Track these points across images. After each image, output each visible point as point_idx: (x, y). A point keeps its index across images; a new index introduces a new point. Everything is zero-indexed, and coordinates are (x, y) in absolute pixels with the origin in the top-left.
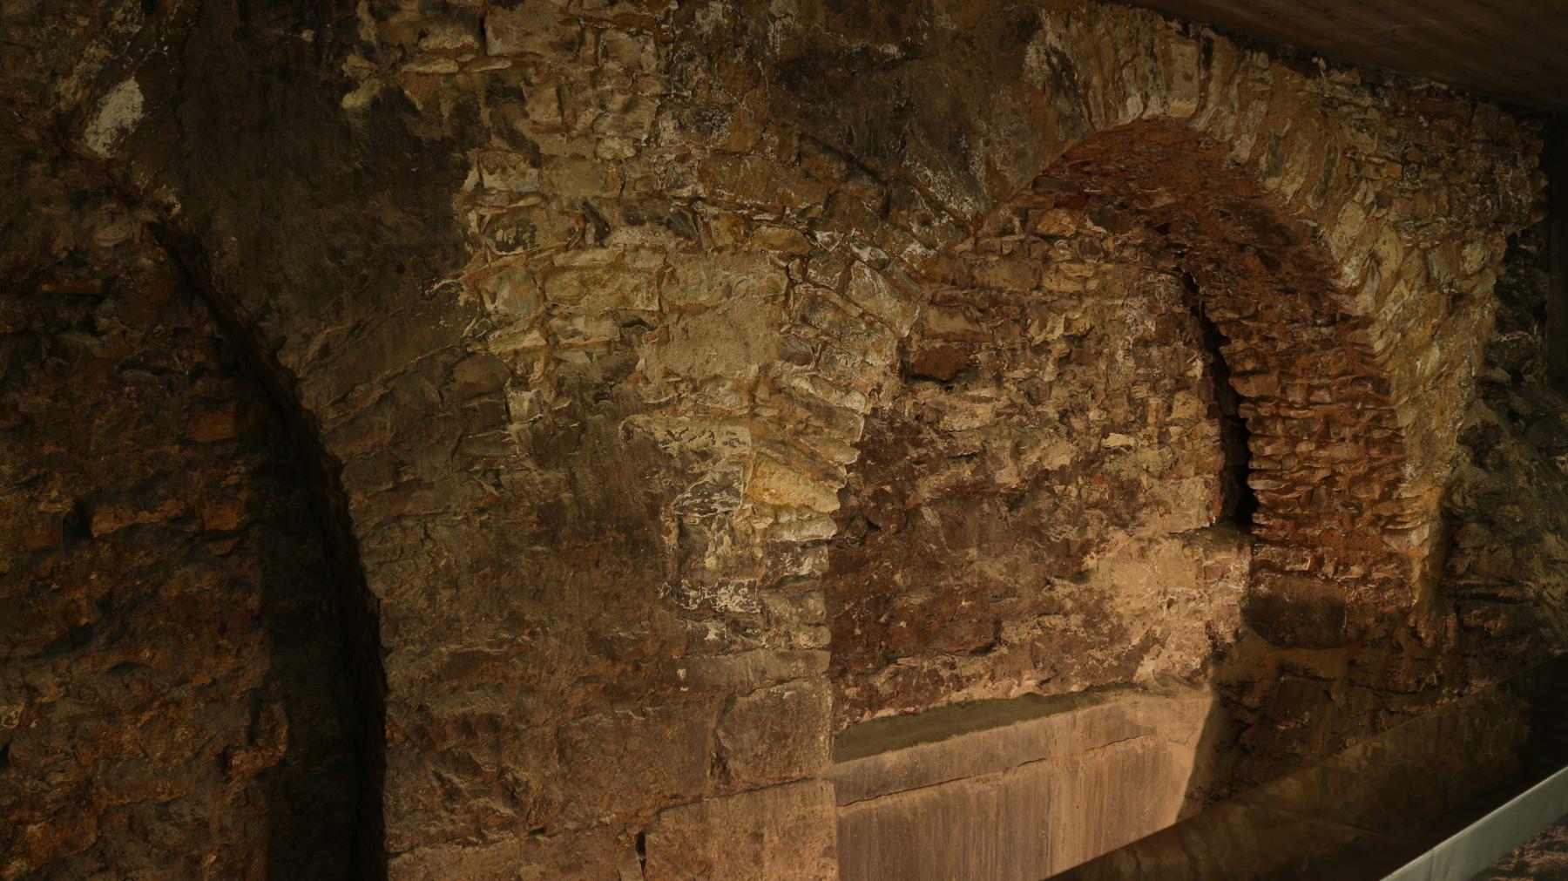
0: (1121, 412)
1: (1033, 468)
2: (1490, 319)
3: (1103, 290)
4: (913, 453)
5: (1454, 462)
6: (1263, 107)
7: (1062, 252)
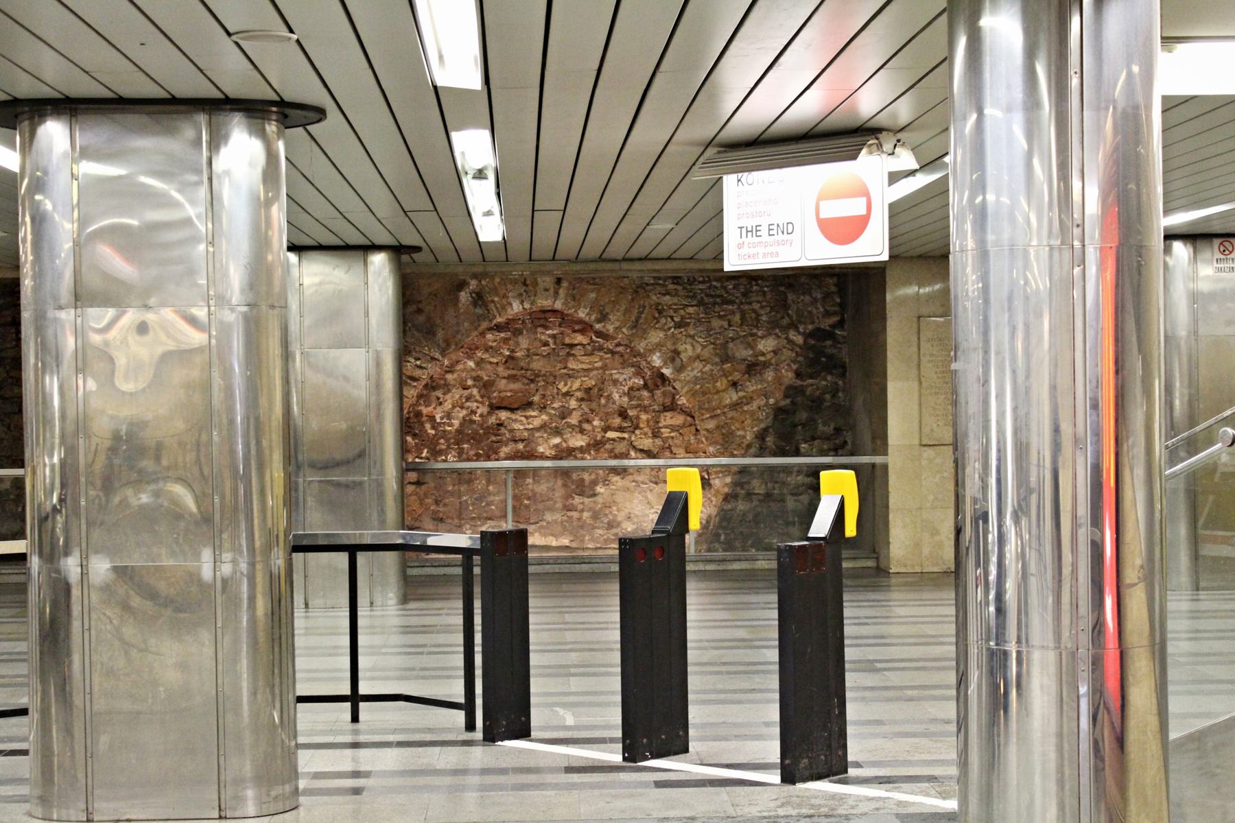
0: (617, 421)
1: (556, 446)
2: (791, 375)
3: (604, 368)
4: (494, 438)
5: (749, 446)
6: (593, 295)
7: (577, 351)
